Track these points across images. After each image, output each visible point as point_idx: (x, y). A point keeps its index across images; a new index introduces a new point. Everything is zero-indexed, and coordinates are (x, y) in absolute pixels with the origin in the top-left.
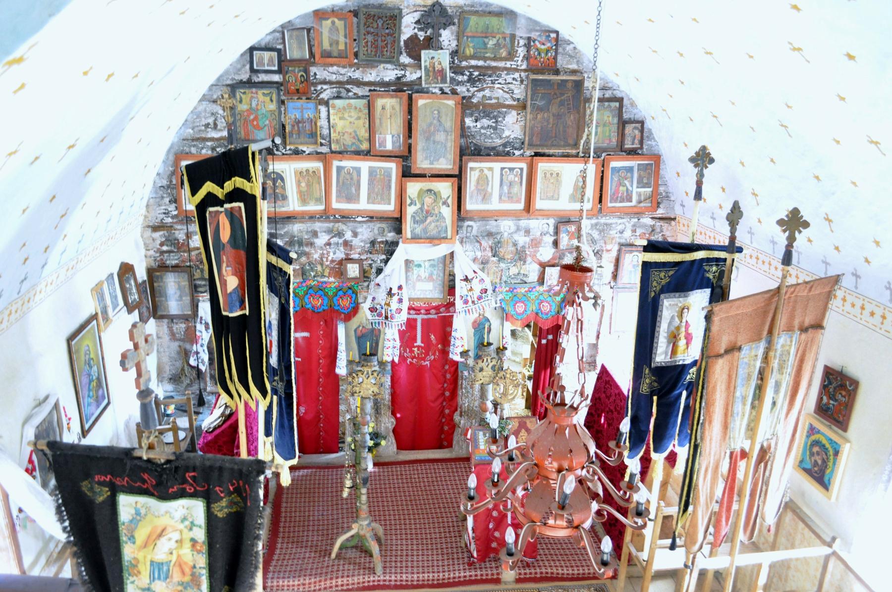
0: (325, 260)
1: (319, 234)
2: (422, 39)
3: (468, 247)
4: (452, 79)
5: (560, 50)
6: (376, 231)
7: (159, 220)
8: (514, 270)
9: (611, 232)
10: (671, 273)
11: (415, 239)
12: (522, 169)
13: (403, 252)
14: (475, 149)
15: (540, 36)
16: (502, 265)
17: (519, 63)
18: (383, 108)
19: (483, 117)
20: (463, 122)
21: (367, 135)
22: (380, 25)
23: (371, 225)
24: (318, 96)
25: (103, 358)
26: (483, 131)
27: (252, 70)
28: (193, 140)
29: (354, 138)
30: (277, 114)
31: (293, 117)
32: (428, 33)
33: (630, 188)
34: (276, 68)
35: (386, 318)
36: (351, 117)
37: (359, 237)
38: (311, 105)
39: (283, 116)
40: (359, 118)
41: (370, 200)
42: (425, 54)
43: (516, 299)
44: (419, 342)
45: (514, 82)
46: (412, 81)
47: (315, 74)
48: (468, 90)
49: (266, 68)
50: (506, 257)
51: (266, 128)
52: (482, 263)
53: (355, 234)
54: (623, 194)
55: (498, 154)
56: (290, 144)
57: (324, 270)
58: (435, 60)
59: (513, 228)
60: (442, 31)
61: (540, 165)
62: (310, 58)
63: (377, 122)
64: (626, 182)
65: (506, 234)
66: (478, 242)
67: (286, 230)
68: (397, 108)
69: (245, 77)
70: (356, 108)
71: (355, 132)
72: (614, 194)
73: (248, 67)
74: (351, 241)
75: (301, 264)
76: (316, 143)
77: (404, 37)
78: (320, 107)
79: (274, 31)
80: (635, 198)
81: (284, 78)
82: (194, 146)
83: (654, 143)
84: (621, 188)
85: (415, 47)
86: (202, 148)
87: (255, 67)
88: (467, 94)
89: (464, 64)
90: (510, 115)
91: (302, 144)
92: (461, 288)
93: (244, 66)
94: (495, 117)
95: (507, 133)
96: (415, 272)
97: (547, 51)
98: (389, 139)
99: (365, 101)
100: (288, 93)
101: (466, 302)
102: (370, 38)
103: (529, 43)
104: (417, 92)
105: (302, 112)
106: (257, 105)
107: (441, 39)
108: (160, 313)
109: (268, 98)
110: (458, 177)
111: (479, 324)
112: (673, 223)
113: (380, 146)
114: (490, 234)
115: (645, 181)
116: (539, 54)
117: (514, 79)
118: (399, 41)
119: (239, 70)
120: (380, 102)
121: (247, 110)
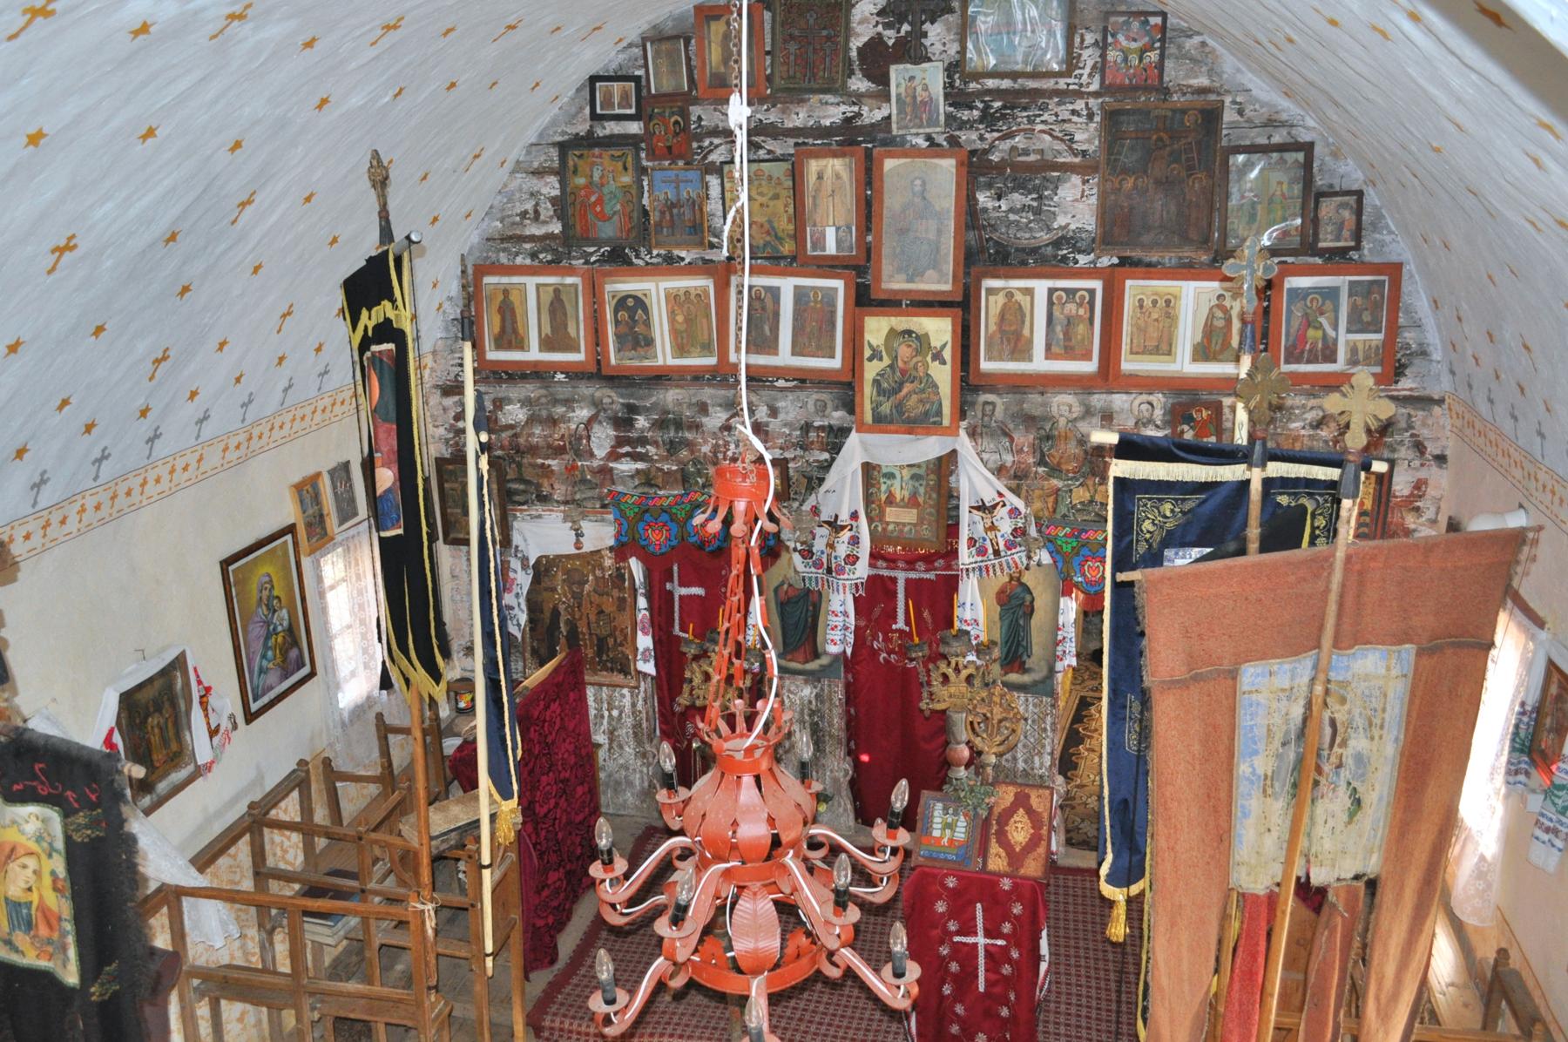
0: (720, 456)
2: (890, 43)
3: (988, 444)
4: (949, 116)
5: (1172, 49)
6: (811, 407)
7: (452, 377)
8: (1080, 495)
9: (1293, 425)
10: (1188, 506)
11: (881, 423)
12: (1092, 292)
13: (856, 449)
14: (997, 252)
15: (1127, 23)
16: (1056, 483)
17: (1085, 79)
18: (820, 177)
19: (1013, 190)
20: (971, 200)
21: (791, 227)
22: (811, 21)
23: (802, 395)
24: (705, 157)
25: (303, 599)
26: (1012, 217)
27: (595, 117)
28: (502, 240)
29: (768, 233)
30: (634, 192)
31: (662, 197)
32: (903, 33)
33: (1331, 333)
34: (632, 111)
35: (829, 571)
36: (761, 194)
37: (781, 416)
38: (693, 175)
39: (646, 194)
40: (776, 197)
41: (797, 350)
42: (897, 73)
43: (1084, 551)
44: (900, 624)
45: (1075, 119)
46: (872, 125)
47: (700, 118)
48: (981, 138)
49: (617, 111)
50: (1064, 467)
51: (616, 218)
52: (1016, 477)
53: (774, 412)
54: (1314, 345)
55: (1044, 260)
56: (658, 245)
58: (916, 82)
59: (1077, 410)
60: (927, 26)
61: (1129, 283)
62: (690, 90)
63: (808, 201)
64: (1321, 319)
65: (1062, 422)
66: (1006, 434)
67: (654, 399)
68: (845, 176)
69: (582, 128)
70: (770, 178)
71: (770, 222)
72: (1294, 346)
73: (587, 110)
74: (767, 424)
76: (701, 244)
77: (856, 43)
78: (708, 178)
79: (630, 45)
80: (1342, 354)
81: (646, 128)
82: (504, 250)
83: (1388, 238)
84: (1311, 333)
85: (877, 60)
86: (517, 254)
87: (598, 111)
88: (979, 145)
89: (973, 86)
90: (1067, 185)
91: (679, 245)
92: (969, 524)
93: (582, 109)
94: (1036, 189)
95: (1061, 220)
96: (883, 488)
97: (1142, 52)
98: (831, 234)
99: (786, 166)
100: (652, 155)
101: (982, 552)
102: (793, 47)
103: (1105, 38)
104: (884, 143)
105: (677, 187)
106: (602, 177)
107: (927, 42)
108: (452, 536)
109: (620, 164)
110: (963, 306)
111: (1010, 598)
112: (1437, 410)
113: (814, 248)
114: (1030, 420)
115: (1366, 317)
116: (1126, 59)
117: (1074, 112)
118: (847, 49)
119: (574, 116)
120: (813, 166)
121: (586, 187)
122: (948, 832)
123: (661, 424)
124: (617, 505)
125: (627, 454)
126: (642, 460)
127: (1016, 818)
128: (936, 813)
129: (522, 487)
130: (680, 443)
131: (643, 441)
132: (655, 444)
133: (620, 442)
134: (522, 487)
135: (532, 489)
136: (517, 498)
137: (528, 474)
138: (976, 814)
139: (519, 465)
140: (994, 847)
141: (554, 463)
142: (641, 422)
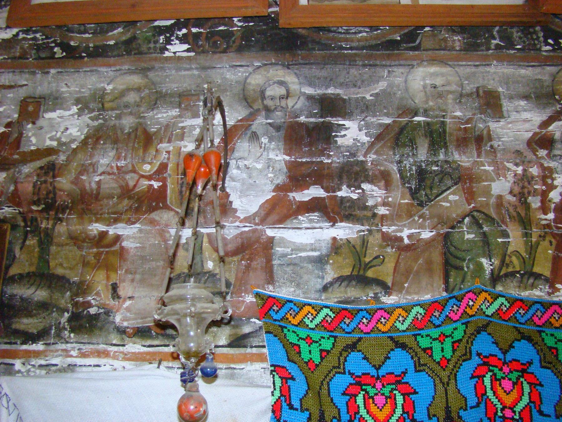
0: (535, 202)
1: (506, 105)
57: (532, 249)
67: (382, 85)
75: (441, 220)
123: (398, 137)
124: (277, 331)
125: (314, 206)
126: (349, 217)
129: (40, 294)
130: (443, 174)
131: (354, 173)
132: (384, 179)
133: (297, 178)
134: (40, 294)
135: (64, 299)
136: (26, 323)
137: (64, 261)
139: (46, 240)
141: (129, 234)
142: (352, 133)
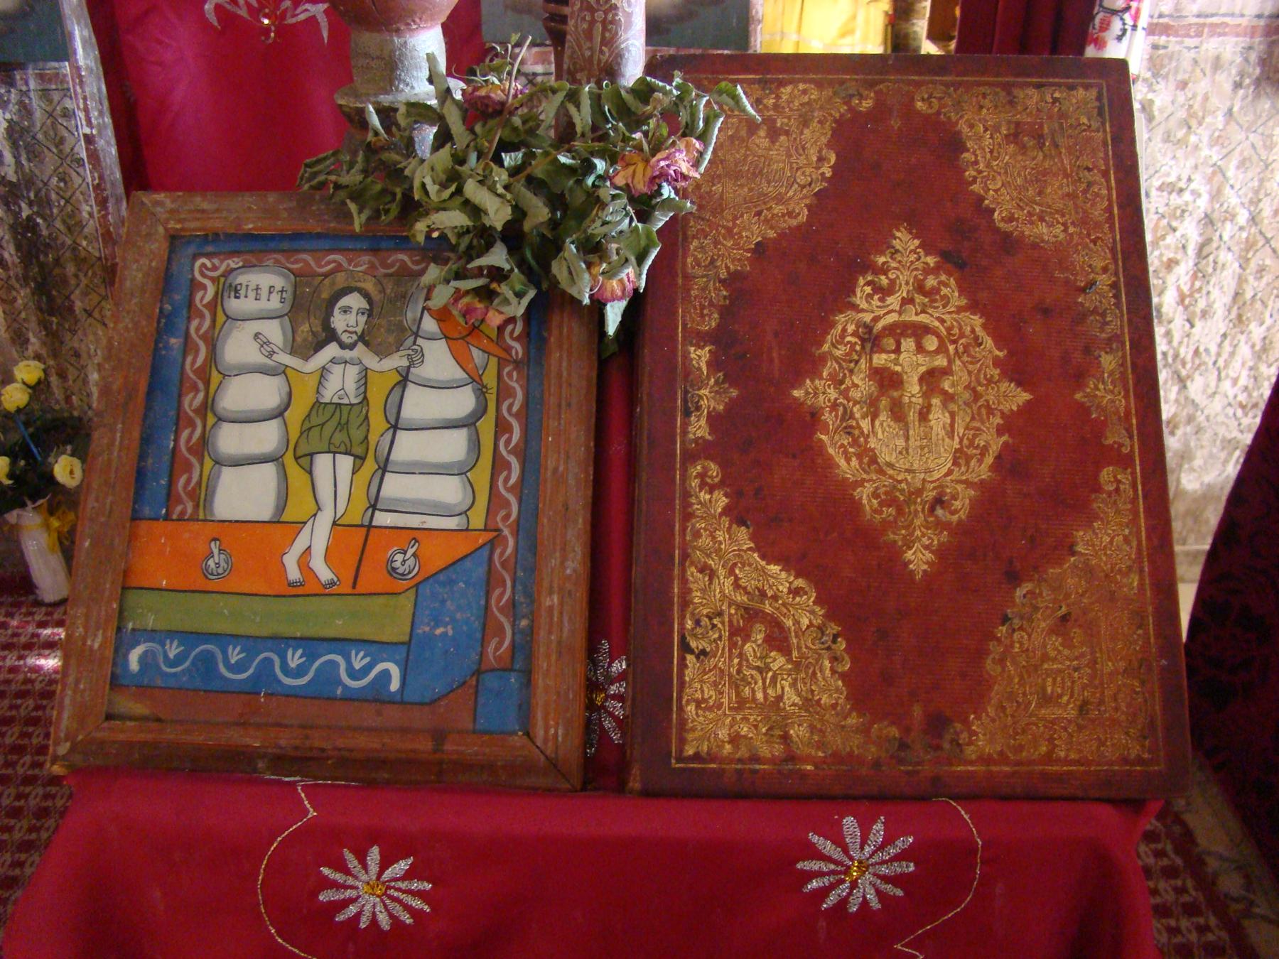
122: (336, 474)
127: (869, 306)
128: (239, 347)
138: (549, 301)
140: (722, 563)
